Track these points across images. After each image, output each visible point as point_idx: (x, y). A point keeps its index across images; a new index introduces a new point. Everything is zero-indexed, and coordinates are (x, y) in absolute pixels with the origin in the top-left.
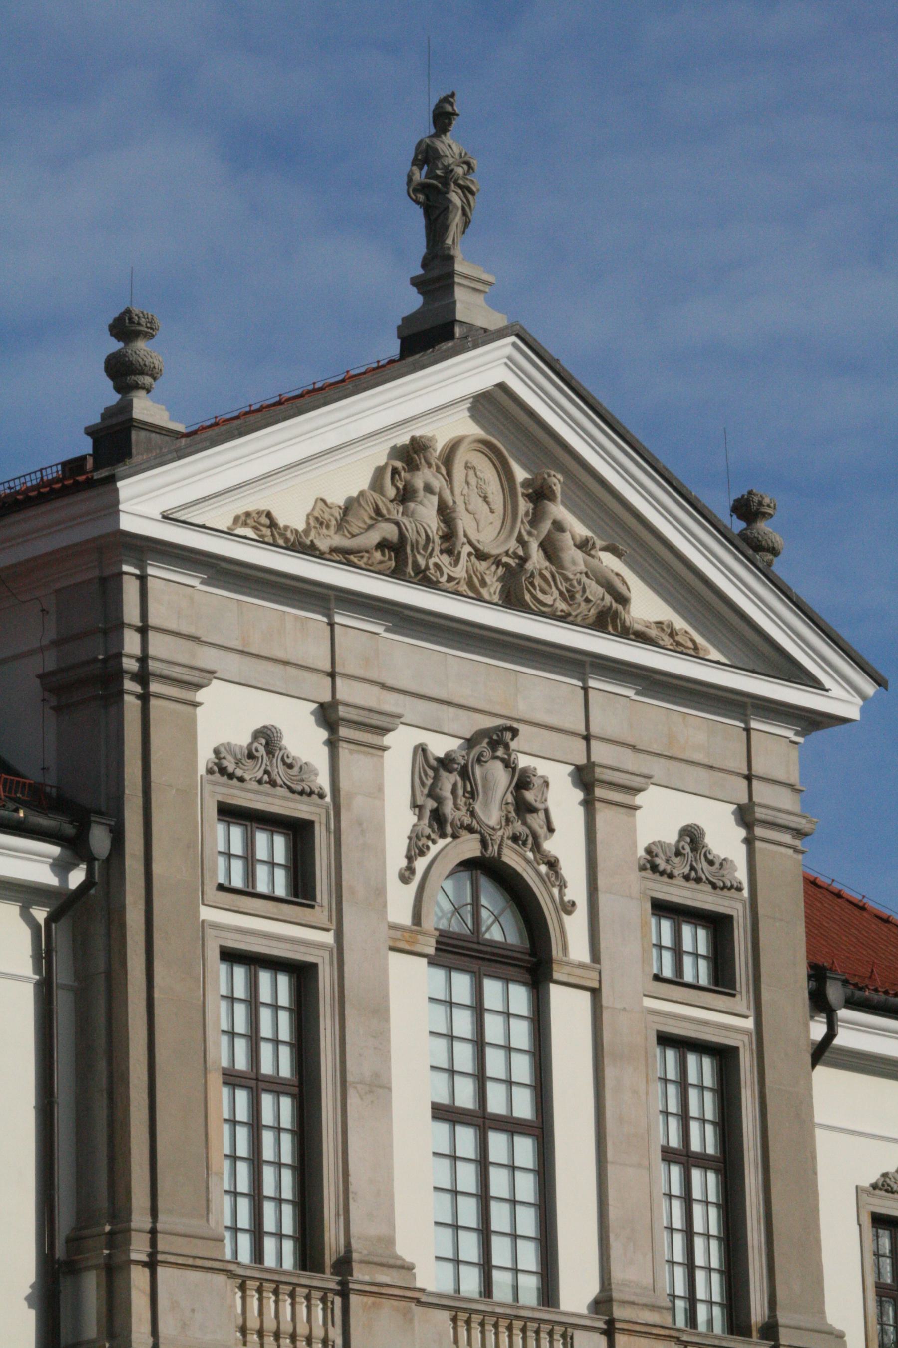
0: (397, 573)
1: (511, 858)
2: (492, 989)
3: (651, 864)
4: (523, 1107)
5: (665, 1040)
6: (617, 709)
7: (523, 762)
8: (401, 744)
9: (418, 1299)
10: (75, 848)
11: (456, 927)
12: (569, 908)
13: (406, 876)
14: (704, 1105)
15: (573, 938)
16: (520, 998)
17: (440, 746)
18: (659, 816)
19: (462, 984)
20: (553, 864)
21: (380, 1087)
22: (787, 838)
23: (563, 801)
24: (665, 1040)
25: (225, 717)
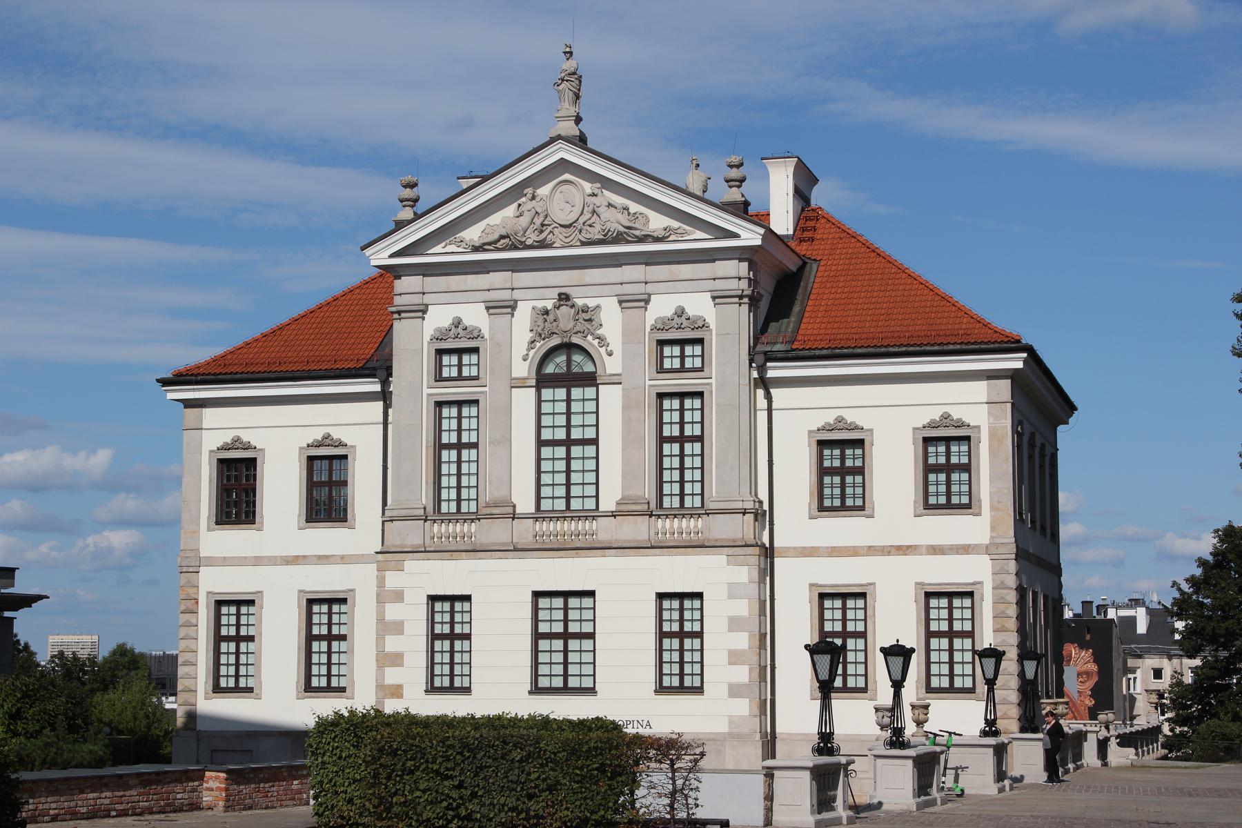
0: (514, 247)
1: (576, 340)
2: (576, 393)
3: (655, 329)
4: (590, 434)
7: (580, 302)
12: (610, 354)
15: (612, 365)
16: (590, 392)
17: (540, 304)
18: (662, 307)
19: (561, 393)
20: (600, 338)
21: (506, 441)
22: (736, 300)
25: (439, 317)
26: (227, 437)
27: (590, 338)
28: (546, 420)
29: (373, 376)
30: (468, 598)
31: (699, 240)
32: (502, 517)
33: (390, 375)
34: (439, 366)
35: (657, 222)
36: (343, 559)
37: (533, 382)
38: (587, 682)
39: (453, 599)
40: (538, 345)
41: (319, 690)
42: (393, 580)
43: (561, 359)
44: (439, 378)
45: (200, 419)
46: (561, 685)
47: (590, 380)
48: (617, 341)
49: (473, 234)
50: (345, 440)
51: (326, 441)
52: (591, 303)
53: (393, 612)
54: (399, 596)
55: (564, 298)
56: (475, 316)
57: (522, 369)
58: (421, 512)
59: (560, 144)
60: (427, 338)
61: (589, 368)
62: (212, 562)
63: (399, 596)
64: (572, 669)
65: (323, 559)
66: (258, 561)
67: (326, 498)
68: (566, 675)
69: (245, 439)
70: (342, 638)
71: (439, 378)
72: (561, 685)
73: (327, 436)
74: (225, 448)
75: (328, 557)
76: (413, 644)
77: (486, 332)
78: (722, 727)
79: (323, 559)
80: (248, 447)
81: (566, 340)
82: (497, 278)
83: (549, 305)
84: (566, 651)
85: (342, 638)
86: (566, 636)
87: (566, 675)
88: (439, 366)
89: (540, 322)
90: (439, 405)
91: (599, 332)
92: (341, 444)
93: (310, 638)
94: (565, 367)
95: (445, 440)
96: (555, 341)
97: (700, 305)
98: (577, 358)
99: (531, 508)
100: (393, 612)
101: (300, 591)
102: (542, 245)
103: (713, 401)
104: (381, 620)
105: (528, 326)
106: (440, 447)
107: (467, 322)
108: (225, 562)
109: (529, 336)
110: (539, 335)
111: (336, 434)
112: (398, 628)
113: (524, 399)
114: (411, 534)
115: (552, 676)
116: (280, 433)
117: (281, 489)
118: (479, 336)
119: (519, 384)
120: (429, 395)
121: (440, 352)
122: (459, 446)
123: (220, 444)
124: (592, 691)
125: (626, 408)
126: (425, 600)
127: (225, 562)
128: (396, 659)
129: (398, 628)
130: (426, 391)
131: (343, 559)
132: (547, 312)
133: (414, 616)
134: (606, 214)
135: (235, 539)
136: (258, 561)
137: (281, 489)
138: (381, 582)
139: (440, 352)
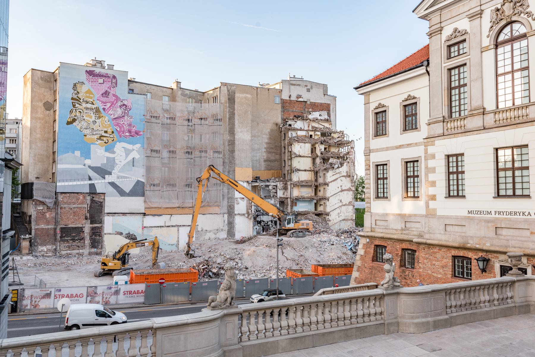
1: (514, 18)
11: (507, 37)
13: (488, 37)
17: (493, 8)
19: (508, 48)
26: (376, 104)
27: (522, 15)
28: (500, 64)
29: (422, 66)
30: (462, 155)
32: (478, 114)
33: (428, 64)
34: (450, 53)
37: (492, 46)
38: (526, 192)
39: (457, 155)
40: (494, 27)
41: (411, 197)
43: (507, 30)
44: (449, 57)
46: (512, 194)
50: (416, 96)
51: (409, 98)
53: (431, 163)
54: (433, 156)
56: (463, 24)
57: (487, 42)
58: (442, 119)
60: (443, 42)
63: (433, 156)
64: (518, 186)
65: (409, 145)
66: (387, 149)
67: (410, 121)
68: (514, 189)
69: (382, 104)
70: (418, 176)
71: (449, 57)
72: (512, 194)
75: (411, 144)
76: (440, 176)
77: (468, 31)
79: (409, 145)
80: (384, 106)
81: (509, 20)
83: (499, 6)
84: (514, 177)
85: (418, 176)
86: (513, 169)
87: (514, 189)
88: (450, 53)
89: (495, 17)
90: (450, 70)
91: (528, 10)
92: (414, 98)
93: (407, 177)
95: (453, 85)
99: (494, 108)
100: (431, 163)
101: (402, 159)
104: (426, 167)
105: (489, 20)
106: (451, 89)
107: (460, 29)
108: (377, 150)
109: (490, 25)
110: (494, 23)
112: (433, 170)
114: (438, 129)
115: (507, 188)
116: (392, 99)
117: (395, 119)
118: (466, 33)
119: (487, 49)
120: (444, 67)
121: (449, 47)
122: (460, 86)
124: (528, 196)
126: (444, 157)
127: (377, 150)
129: (433, 170)
130: (443, 65)
132: (498, 10)
133: (440, 164)
136: (387, 149)
137: (395, 119)
138: (426, 151)
139: (449, 47)
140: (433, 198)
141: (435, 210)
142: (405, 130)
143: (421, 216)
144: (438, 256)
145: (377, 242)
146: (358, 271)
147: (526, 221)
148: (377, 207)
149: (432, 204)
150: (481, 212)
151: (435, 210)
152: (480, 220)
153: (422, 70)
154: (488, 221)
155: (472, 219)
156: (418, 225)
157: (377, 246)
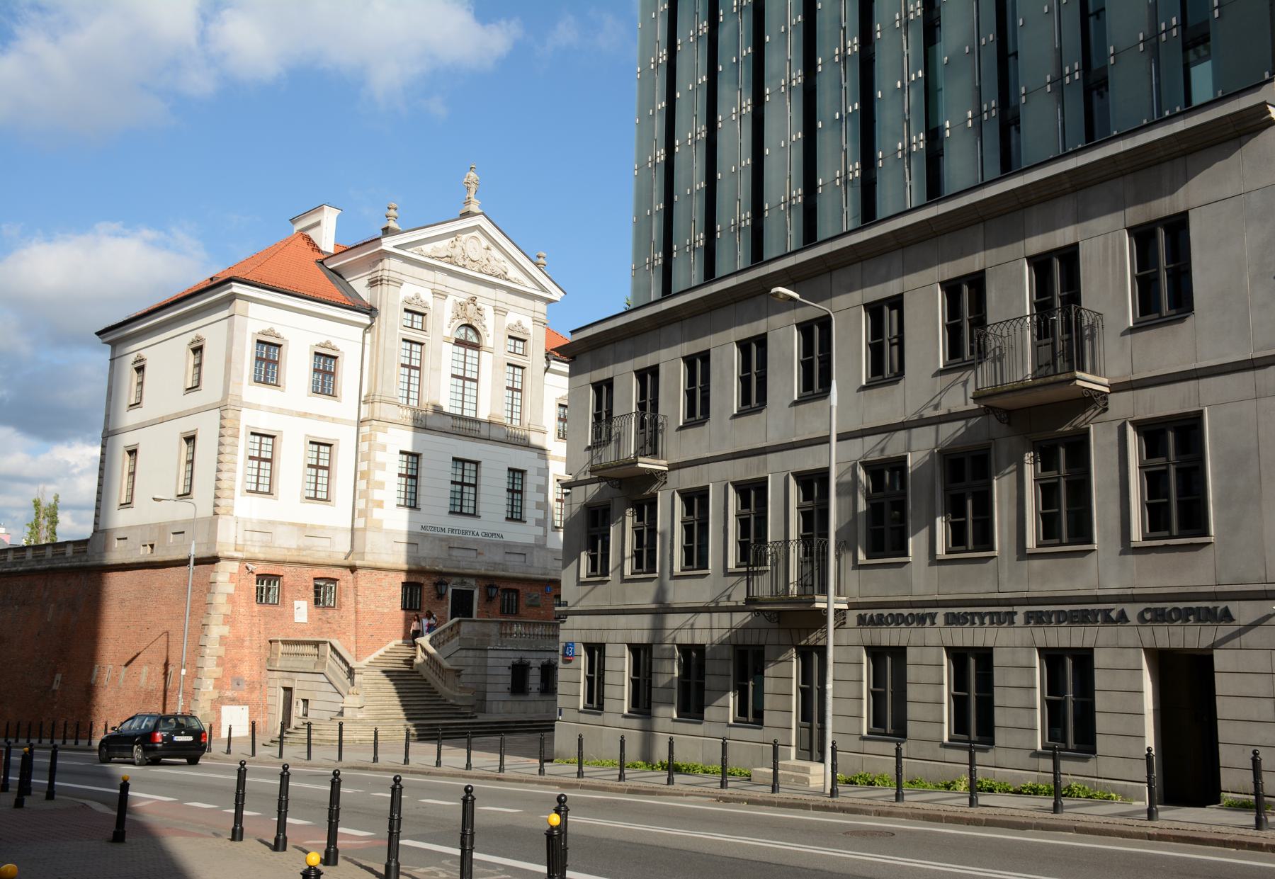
1: (474, 324)
2: (469, 352)
5: (509, 365)
6: (502, 295)
8: (450, 299)
9: (445, 414)
10: (372, 318)
14: (518, 378)
15: (488, 342)
16: (475, 353)
17: (459, 300)
18: (511, 319)
19: (462, 350)
21: (438, 370)
23: (488, 312)
24: (509, 365)
25: (408, 291)
26: (266, 327)
31: (530, 287)
35: (513, 273)
36: (334, 420)
42: (381, 438)
45: (247, 309)
47: (476, 347)
48: (493, 332)
49: (427, 248)
52: (483, 306)
54: (384, 448)
55: (473, 300)
56: (427, 296)
59: (482, 217)
60: (401, 299)
61: (475, 340)
62: (249, 406)
65: (321, 417)
73: (328, 342)
74: (263, 333)
78: (532, 541)
79: (321, 417)
82: (440, 277)
94: (469, 340)
96: (465, 322)
97: (527, 323)
98: (470, 333)
102: (464, 266)
103: (528, 371)
109: (451, 315)
111: (334, 343)
112: (382, 467)
113: (449, 350)
117: (297, 366)
123: (260, 330)
125: (494, 366)
128: (381, 485)
131: (334, 420)
134: (493, 262)
135: (264, 394)
137: (297, 366)
140: (380, 504)
141: (381, 521)
142: (334, 396)
143: (335, 529)
144: (385, 583)
145: (260, 569)
146: (225, 623)
147: (475, 540)
148: (246, 508)
149: (377, 513)
150: (435, 529)
151: (381, 521)
152: (434, 538)
153: (365, 319)
154: (442, 539)
155: (425, 536)
156: (326, 542)
157: (261, 577)
